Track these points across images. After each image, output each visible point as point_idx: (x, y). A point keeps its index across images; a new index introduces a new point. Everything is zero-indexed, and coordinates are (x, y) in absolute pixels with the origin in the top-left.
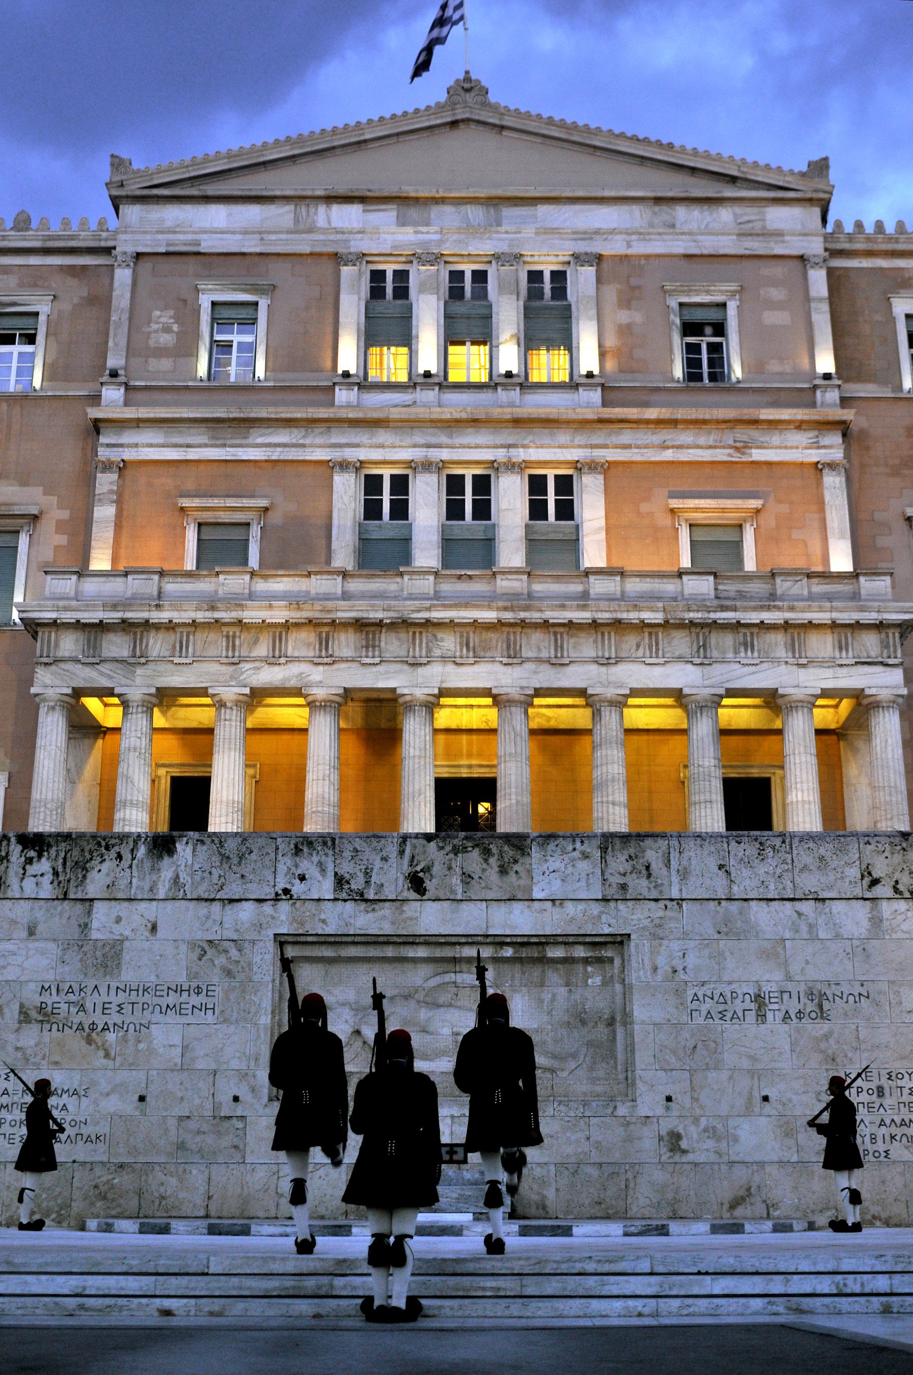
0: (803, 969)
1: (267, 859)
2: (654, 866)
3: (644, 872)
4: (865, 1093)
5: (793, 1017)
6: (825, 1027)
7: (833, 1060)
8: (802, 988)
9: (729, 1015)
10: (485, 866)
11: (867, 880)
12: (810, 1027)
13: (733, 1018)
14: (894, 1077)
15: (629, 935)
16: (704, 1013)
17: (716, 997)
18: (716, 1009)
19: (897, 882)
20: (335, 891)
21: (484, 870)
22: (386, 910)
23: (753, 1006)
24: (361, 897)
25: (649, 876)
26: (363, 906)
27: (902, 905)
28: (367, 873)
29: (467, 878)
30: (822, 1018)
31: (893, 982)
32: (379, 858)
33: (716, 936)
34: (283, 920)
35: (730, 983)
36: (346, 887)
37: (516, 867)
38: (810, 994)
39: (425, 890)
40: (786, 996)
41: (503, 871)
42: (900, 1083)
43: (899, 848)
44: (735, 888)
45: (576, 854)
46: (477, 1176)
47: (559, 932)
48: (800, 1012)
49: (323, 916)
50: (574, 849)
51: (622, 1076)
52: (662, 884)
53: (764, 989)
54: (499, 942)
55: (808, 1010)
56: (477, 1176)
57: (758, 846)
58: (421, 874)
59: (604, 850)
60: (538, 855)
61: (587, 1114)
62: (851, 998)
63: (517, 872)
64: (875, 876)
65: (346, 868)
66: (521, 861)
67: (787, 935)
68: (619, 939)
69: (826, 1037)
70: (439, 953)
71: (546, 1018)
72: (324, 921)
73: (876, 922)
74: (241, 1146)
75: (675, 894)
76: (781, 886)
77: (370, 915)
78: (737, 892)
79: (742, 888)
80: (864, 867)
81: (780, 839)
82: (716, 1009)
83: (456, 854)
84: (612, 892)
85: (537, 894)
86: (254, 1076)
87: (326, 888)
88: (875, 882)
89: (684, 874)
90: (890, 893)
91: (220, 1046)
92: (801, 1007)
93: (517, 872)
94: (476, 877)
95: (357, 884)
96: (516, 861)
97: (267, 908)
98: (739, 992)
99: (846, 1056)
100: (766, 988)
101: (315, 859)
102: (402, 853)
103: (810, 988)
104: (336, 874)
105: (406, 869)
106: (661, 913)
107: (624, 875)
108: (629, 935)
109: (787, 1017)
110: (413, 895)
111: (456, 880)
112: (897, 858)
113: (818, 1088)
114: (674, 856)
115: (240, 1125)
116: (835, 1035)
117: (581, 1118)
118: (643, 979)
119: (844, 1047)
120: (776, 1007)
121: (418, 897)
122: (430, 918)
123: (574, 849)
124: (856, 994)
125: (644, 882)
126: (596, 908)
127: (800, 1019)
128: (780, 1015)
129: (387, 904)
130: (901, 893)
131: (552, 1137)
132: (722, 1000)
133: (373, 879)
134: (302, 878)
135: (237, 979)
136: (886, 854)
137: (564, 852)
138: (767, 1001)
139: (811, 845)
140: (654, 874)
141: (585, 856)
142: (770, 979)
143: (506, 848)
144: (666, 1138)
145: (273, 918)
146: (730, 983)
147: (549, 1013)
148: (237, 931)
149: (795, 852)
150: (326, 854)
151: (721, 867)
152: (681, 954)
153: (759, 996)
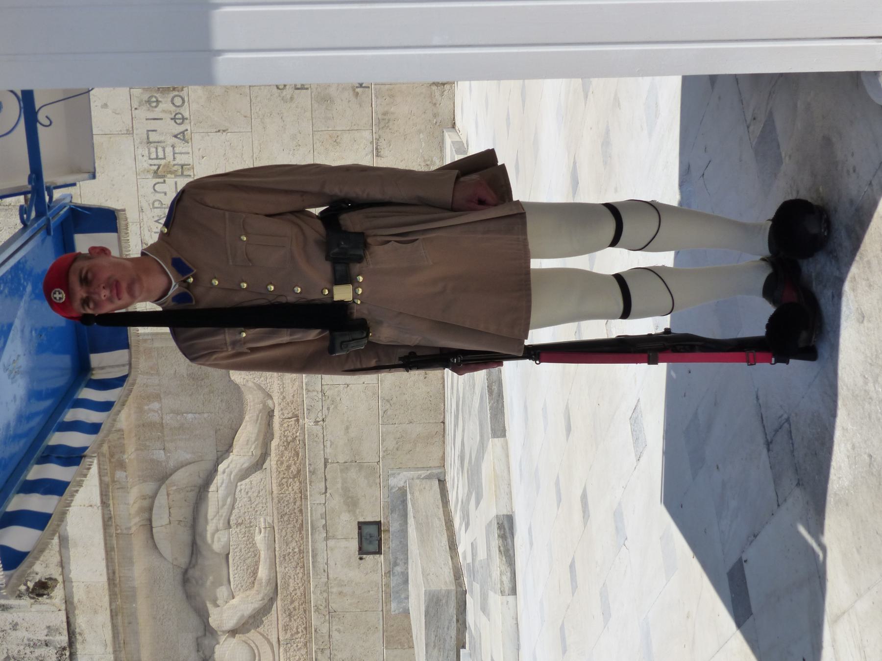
0: (115, 112)
8: (142, 113)
12: (194, 106)
22: (81, 621)
32: (13, 634)
35: (141, 210)
39: (50, 579)
40: (153, 137)
46: (395, 516)
48: (174, 119)
53: (146, 165)
55: (173, 108)
56: (395, 516)
58: (31, 585)
77: (89, 636)
98: (152, 197)
100: (144, 163)
102: (5, 608)
105: (26, 601)
109: (181, 136)
110: (58, 593)
117: (324, 394)
120: (169, 150)
121: (60, 586)
128: (181, 147)
131: (347, 428)
133: (43, 638)
138: (163, 162)
146: (141, 210)
153: (156, 172)
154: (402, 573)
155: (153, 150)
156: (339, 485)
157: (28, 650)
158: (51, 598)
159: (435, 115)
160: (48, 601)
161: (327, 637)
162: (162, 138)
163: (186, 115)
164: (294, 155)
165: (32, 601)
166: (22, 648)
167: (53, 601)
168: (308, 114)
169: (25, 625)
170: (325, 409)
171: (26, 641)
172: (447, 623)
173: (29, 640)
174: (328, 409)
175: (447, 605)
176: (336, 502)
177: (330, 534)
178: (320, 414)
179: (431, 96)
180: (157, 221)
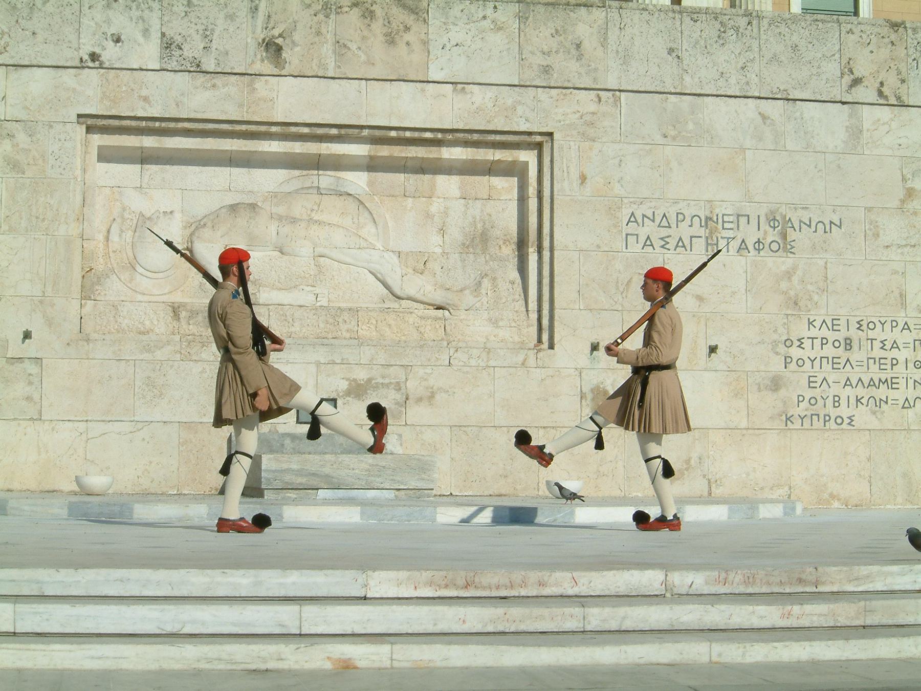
1: (68, 11)
2: (586, 45)
3: (573, 52)
4: (830, 344)
5: (751, 248)
6: (787, 262)
7: (796, 303)
9: (672, 243)
10: (366, 33)
11: (847, 79)
13: (677, 246)
14: (864, 327)
15: (551, 134)
16: (642, 239)
17: (658, 220)
18: (656, 234)
19: (882, 84)
20: (162, 58)
21: (364, 38)
23: (702, 232)
24: (198, 69)
25: (580, 58)
26: (201, 78)
27: (884, 113)
28: (207, 35)
29: (341, 46)
30: (785, 250)
31: (869, 209)
32: (222, 15)
33: (661, 140)
34: (92, 93)
35: (676, 202)
36: (179, 52)
37: (408, 37)
38: (772, 219)
40: (743, 220)
41: (391, 40)
42: (871, 334)
43: (886, 40)
44: (687, 79)
45: (486, 24)
47: (461, 126)
48: (759, 242)
49: (144, 93)
50: (484, 17)
51: (534, 316)
52: (596, 70)
53: (717, 211)
54: (380, 136)
55: (769, 240)
57: (718, 26)
58: (279, 41)
59: (522, 18)
60: (437, 23)
61: (492, 363)
62: (820, 226)
63: (408, 44)
64: (857, 74)
65: (175, 29)
66: (414, 28)
67: (748, 143)
68: (538, 138)
69: (789, 275)
70: (297, 148)
71: (436, 239)
72: (146, 99)
73: (855, 132)
74: (36, 397)
75: (612, 83)
76: (744, 80)
78: (690, 84)
79: (696, 80)
80: (844, 62)
81: (746, 19)
82: (656, 234)
83: (327, 17)
84: (531, 76)
85: (433, 76)
86: (53, 305)
87: (148, 53)
88: (856, 82)
89: (626, 58)
90: (873, 97)
91: (5, 264)
92: (760, 235)
93: (408, 44)
94: (353, 47)
95: (193, 49)
96: (407, 29)
97: (67, 77)
99: (811, 299)
101: (135, 13)
103: (772, 212)
104: (163, 35)
106: (593, 107)
107: (549, 54)
108: (551, 134)
110: (267, 68)
111: (327, 50)
112: (884, 53)
113: (775, 337)
114: (613, 34)
115: (33, 369)
116: (799, 273)
118: (568, 193)
119: (810, 287)
120: (730, 234)
121: (276, 71)
122: (289, 99)
123: (484, 17)
124: (827, 223)
125: (573, 65)
126: (509, 97)
127: (759, 250)
128: (734, 245)
129: (233, 78)
130: (886, 98)
132: (664, 223)
133: (214, 45)
134: (118, 40)
135: (29, 174)
136: (870, 48)
137: (470, 20)
139: (783, 28)
140: (587, 56)
141: (498, 28)
142: (726, 198)
143: (395, 11)
144: (590, 396)
145: (74, 90)
146: (676, 202)
147: (442, 231)
148: (26, 108)
149: (763, 37)
150: (150, 9)
151: (671, 51)
152: (617, 161)
153: (711, 219)
154: (283, 445)
155: (731, 219)
156: (381, 380)
157: (201, 28)
158: (263, 61)
159: (762, 489)
160: (259, 57)
161: (194, 358)
162: (741, 228)
163: (762, 253)
164: (725, 351)
165: (260, 41)
166: (205, 22)
167: (259, 62)
168: (762, 368)
169: (231, 29)
170: (468, 369)
171: (210, 27)
172: (398, 478)
173: (213, 30)
174: (467, 372)
175: (418, 480)
176: (361, 375)
177: (323, 367)
178: (462, 364)
179: (779, 486)
180: (664, 215)
